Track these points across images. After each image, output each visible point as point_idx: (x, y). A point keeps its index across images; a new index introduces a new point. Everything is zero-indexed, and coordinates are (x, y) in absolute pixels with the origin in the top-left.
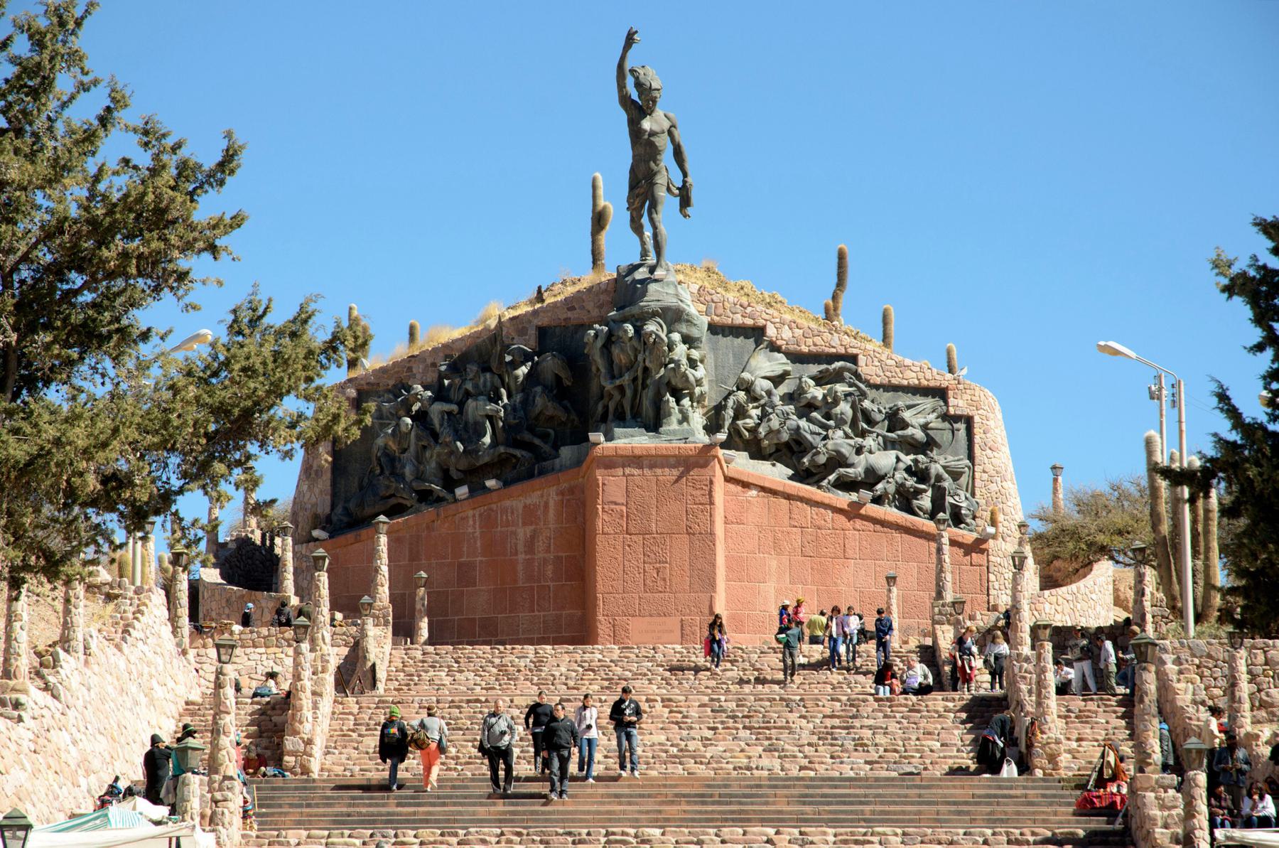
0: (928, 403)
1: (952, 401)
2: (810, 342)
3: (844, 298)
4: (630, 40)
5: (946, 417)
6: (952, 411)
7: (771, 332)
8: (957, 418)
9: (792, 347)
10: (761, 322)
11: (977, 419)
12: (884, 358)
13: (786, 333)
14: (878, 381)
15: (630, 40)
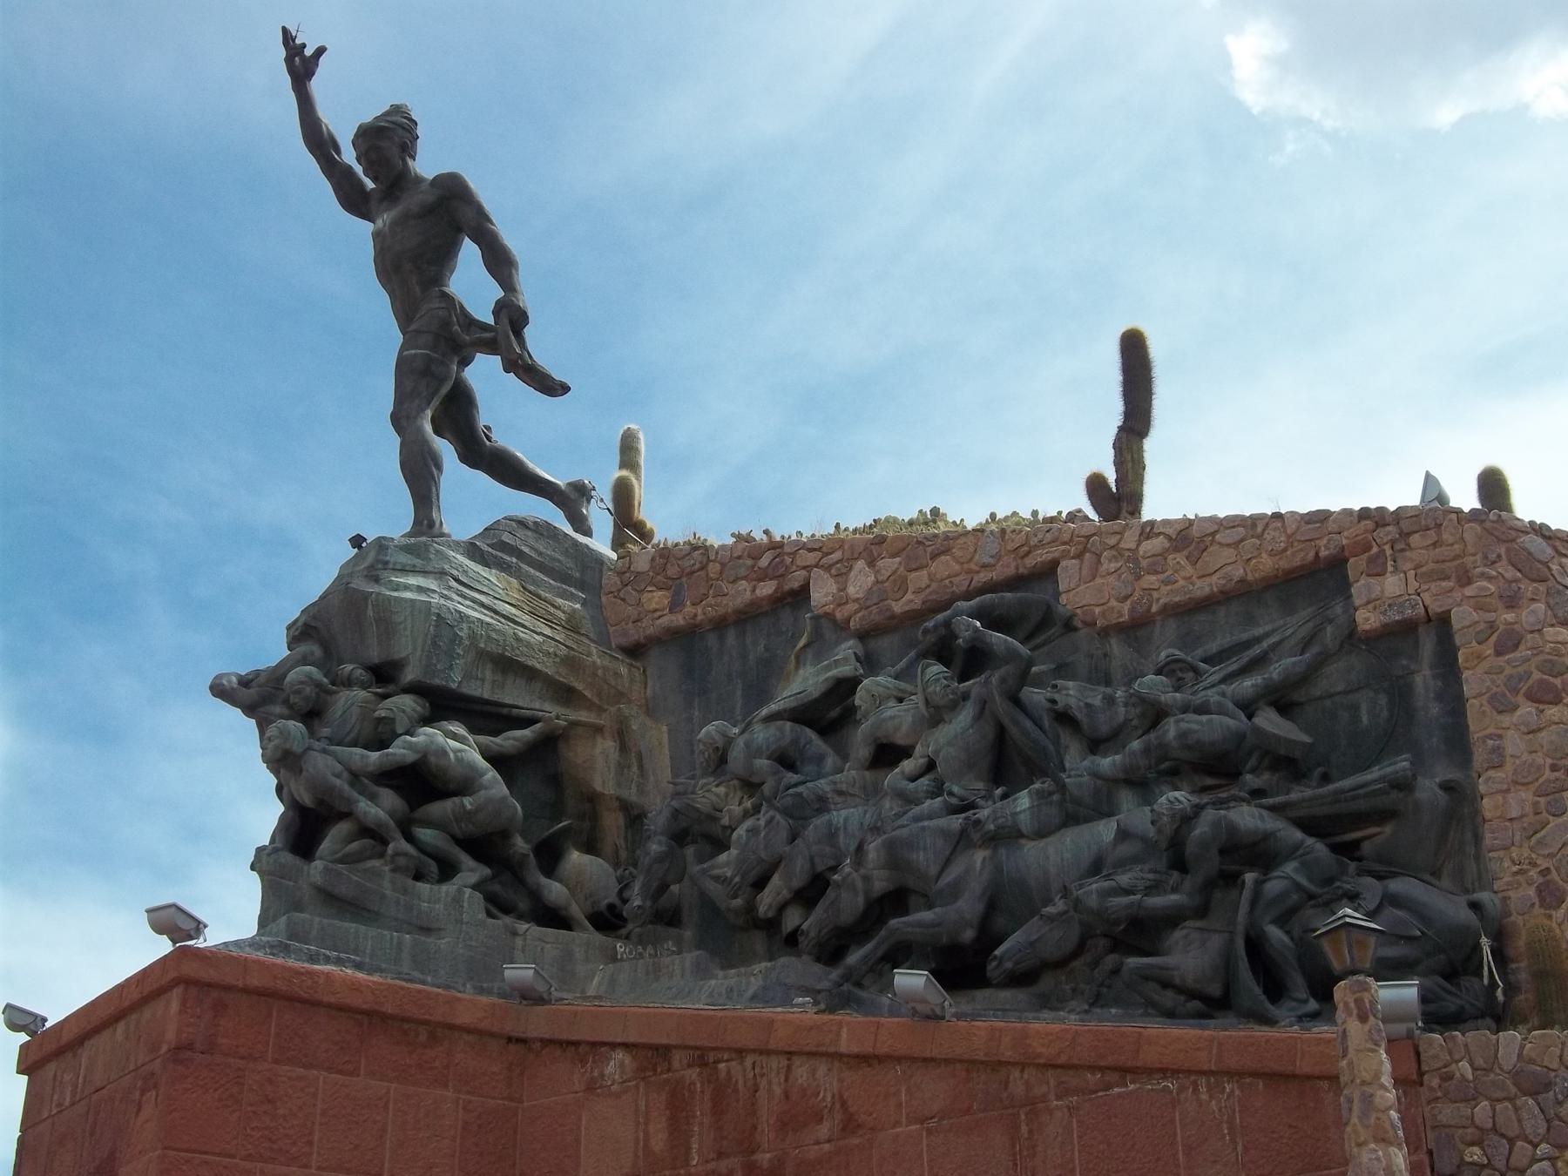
0: (1297, 623)
1: (1360, 589)
2: (919, 579)
3: (1153, 447)
4: (301, 65)
5: (1352, 638)
6: (1367, 620)
7: (822, 593)
8: (1403, 632)
9: (875, 616)
10: (794, 583)
11: (1462, 617)
12: (1129, 541)
13: (861, 581)
14: (1125, 612)
15: (301, 65)
